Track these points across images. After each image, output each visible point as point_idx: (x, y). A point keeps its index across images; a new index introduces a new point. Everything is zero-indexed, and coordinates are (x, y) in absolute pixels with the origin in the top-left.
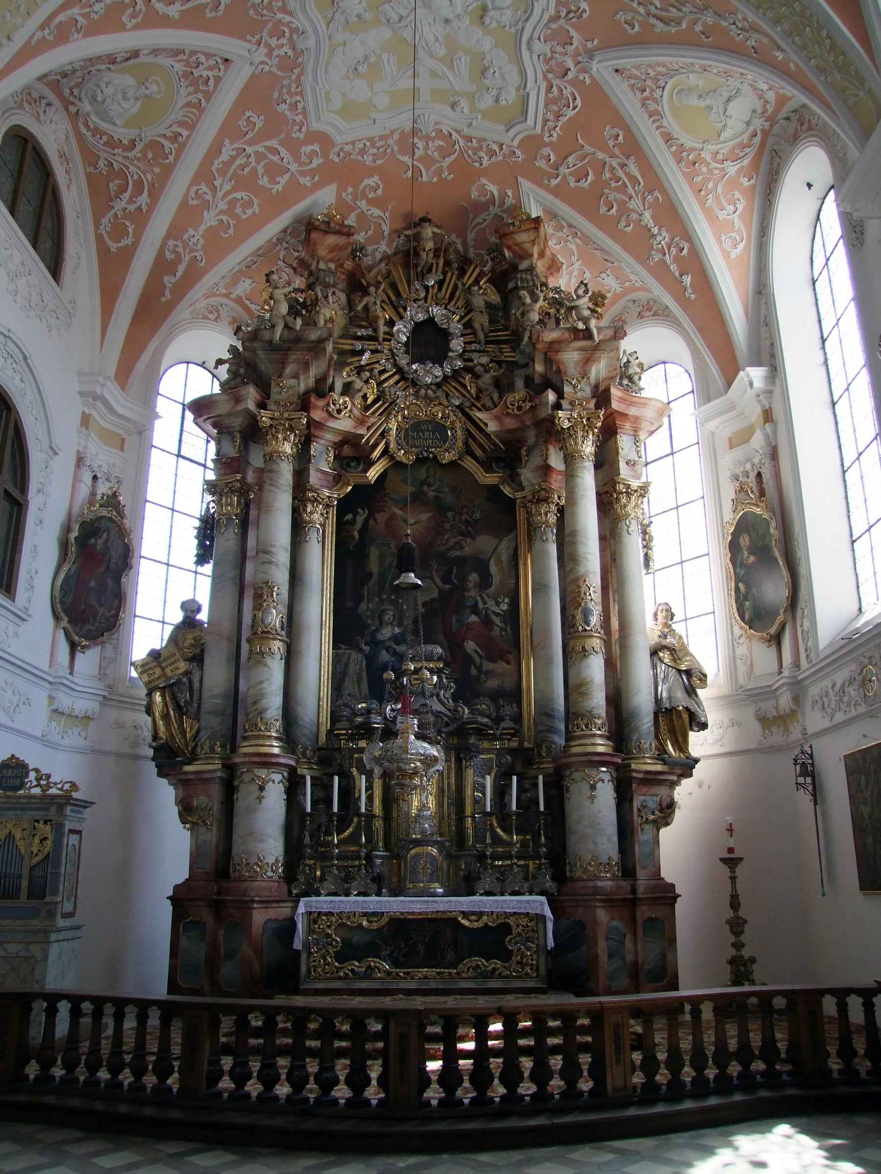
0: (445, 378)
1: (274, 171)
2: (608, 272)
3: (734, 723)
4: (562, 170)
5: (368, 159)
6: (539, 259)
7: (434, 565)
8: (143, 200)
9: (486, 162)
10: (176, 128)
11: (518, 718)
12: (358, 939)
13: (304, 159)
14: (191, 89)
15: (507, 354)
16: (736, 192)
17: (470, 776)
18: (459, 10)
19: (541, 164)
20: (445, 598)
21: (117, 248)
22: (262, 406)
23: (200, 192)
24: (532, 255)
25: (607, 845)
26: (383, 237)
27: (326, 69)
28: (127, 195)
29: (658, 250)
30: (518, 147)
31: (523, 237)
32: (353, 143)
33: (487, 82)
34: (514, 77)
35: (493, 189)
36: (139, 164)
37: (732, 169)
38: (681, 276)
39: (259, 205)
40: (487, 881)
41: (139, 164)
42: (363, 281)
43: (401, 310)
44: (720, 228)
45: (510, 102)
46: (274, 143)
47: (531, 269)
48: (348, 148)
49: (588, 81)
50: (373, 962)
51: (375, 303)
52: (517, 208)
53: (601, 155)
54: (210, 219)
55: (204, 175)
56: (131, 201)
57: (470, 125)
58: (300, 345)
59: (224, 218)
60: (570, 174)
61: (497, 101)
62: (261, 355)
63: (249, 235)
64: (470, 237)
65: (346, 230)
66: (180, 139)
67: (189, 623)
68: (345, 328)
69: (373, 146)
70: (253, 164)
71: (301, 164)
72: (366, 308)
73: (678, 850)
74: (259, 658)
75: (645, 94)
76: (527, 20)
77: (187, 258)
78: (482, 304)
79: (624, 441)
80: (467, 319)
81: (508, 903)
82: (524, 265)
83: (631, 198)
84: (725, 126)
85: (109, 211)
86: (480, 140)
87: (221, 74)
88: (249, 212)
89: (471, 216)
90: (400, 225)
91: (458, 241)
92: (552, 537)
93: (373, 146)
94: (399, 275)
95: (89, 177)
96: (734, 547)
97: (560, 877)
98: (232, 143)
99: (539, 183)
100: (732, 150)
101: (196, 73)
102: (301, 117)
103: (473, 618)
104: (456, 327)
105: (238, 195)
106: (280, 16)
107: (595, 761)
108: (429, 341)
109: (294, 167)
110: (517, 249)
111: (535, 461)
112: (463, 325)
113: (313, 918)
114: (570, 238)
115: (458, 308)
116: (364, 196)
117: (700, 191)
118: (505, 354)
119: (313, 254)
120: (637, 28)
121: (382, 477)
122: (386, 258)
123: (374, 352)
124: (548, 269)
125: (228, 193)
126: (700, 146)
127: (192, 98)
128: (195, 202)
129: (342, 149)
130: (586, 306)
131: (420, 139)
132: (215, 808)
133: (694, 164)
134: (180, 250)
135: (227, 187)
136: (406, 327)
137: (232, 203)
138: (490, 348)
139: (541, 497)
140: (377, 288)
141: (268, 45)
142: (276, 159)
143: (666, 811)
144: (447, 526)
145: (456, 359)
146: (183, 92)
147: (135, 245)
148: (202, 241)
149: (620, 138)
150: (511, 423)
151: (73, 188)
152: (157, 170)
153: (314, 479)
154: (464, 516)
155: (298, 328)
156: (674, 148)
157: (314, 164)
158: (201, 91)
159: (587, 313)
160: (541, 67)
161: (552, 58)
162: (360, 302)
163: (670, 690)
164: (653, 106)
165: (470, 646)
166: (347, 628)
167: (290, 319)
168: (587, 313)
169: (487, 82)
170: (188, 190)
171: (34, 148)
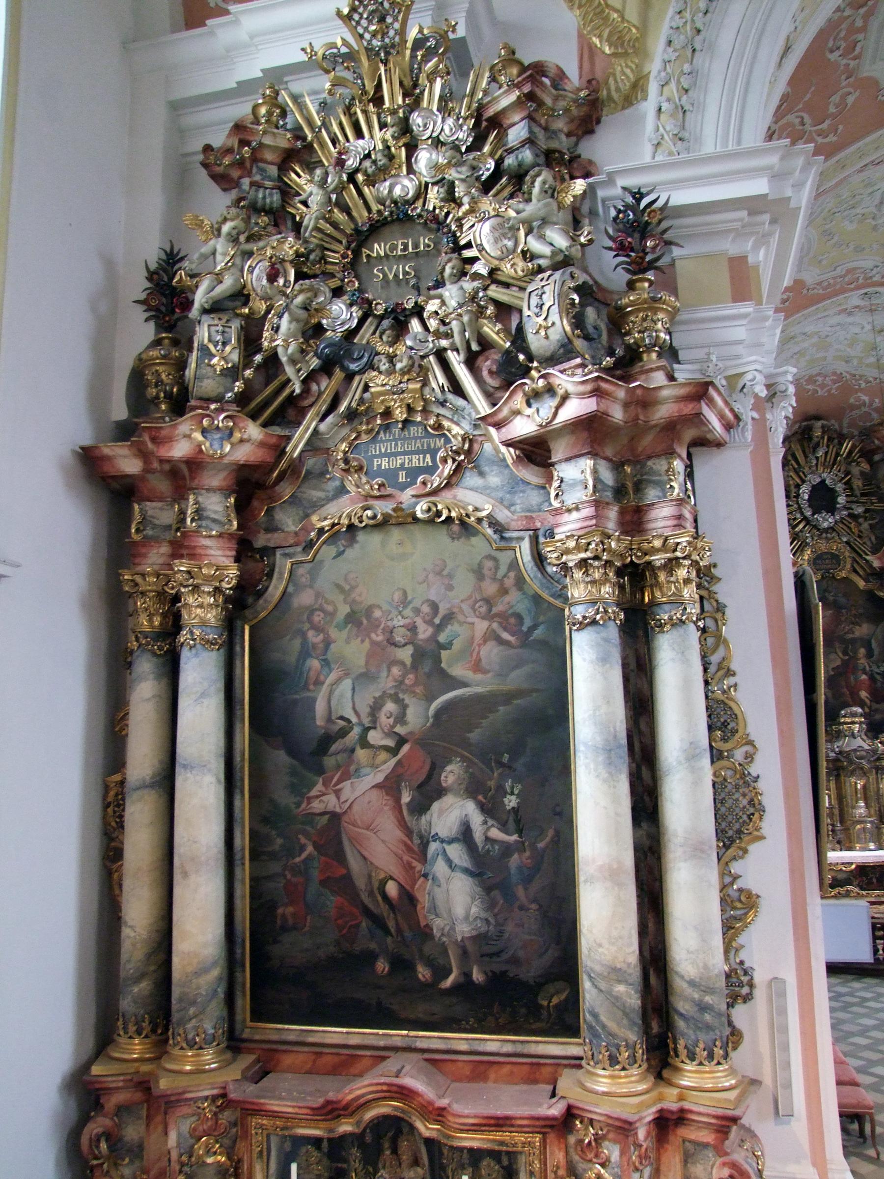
0: (836, 522)
7: (837, 645)
9: (863, 385)
12: (840, 876)
20: (845, 664)
35: (866, 399)
50: (849, 887)
86: (861, 376)
103: (864, 677)
104: (840, 487)
144: (843, 619)
154: (854, 612)
165: (864, 694)
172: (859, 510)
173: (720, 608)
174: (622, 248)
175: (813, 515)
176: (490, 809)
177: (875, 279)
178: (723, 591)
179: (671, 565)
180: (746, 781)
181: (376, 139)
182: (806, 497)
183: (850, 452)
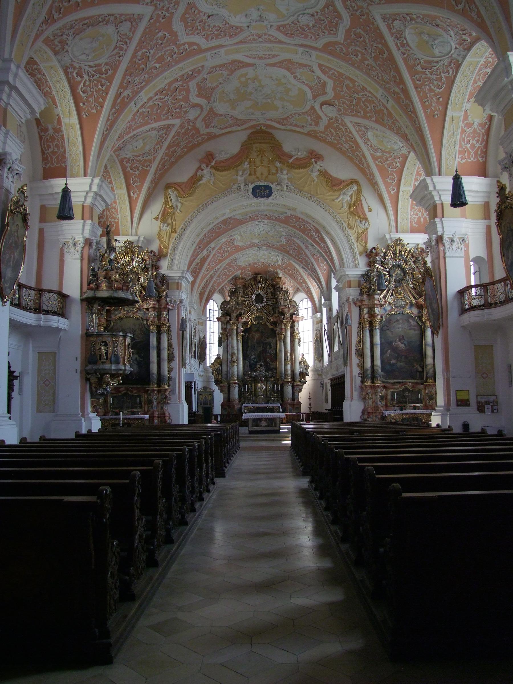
3: (314, 375)
8: (208, 283)
11: (276, 373)
15: (275, 302)
17: (268, 385)
22: (230, 320)
25: (290, 396)
31: (278, 280)
40: (271, 401)
47: (279, 287)
52: (277, 273)
54: (218, 282)
55: (219, 276)
64: (268, 276)
67: (218, 358)
73: (303, 396)
74: (233, 366)
79: (296, 324)
81: (274, 405)
82: (278, 286)
92: (283, 341)
96: (315, 343)
97: (282, 401)
104: (265, 296)
107: (288, 382)
108: (259, 299)
111: (280, 327)
113: (245, 407)
119: (237, 283)
121: (251, 326)
132: (226, 390)
139: (281, 334)
143: (300, 390)
150: (275, 320)
153: (239, 331)
163: (303, 369)
165: (268, 359)
166: (245, 357)
172: (270, 303)
173: (171, 331)
174: (160, 282)
176: (140, 356)
178: (171, 329)
179: (163, 325)
180: (173, 353)
181: (127, 259)
183: (269, 285)
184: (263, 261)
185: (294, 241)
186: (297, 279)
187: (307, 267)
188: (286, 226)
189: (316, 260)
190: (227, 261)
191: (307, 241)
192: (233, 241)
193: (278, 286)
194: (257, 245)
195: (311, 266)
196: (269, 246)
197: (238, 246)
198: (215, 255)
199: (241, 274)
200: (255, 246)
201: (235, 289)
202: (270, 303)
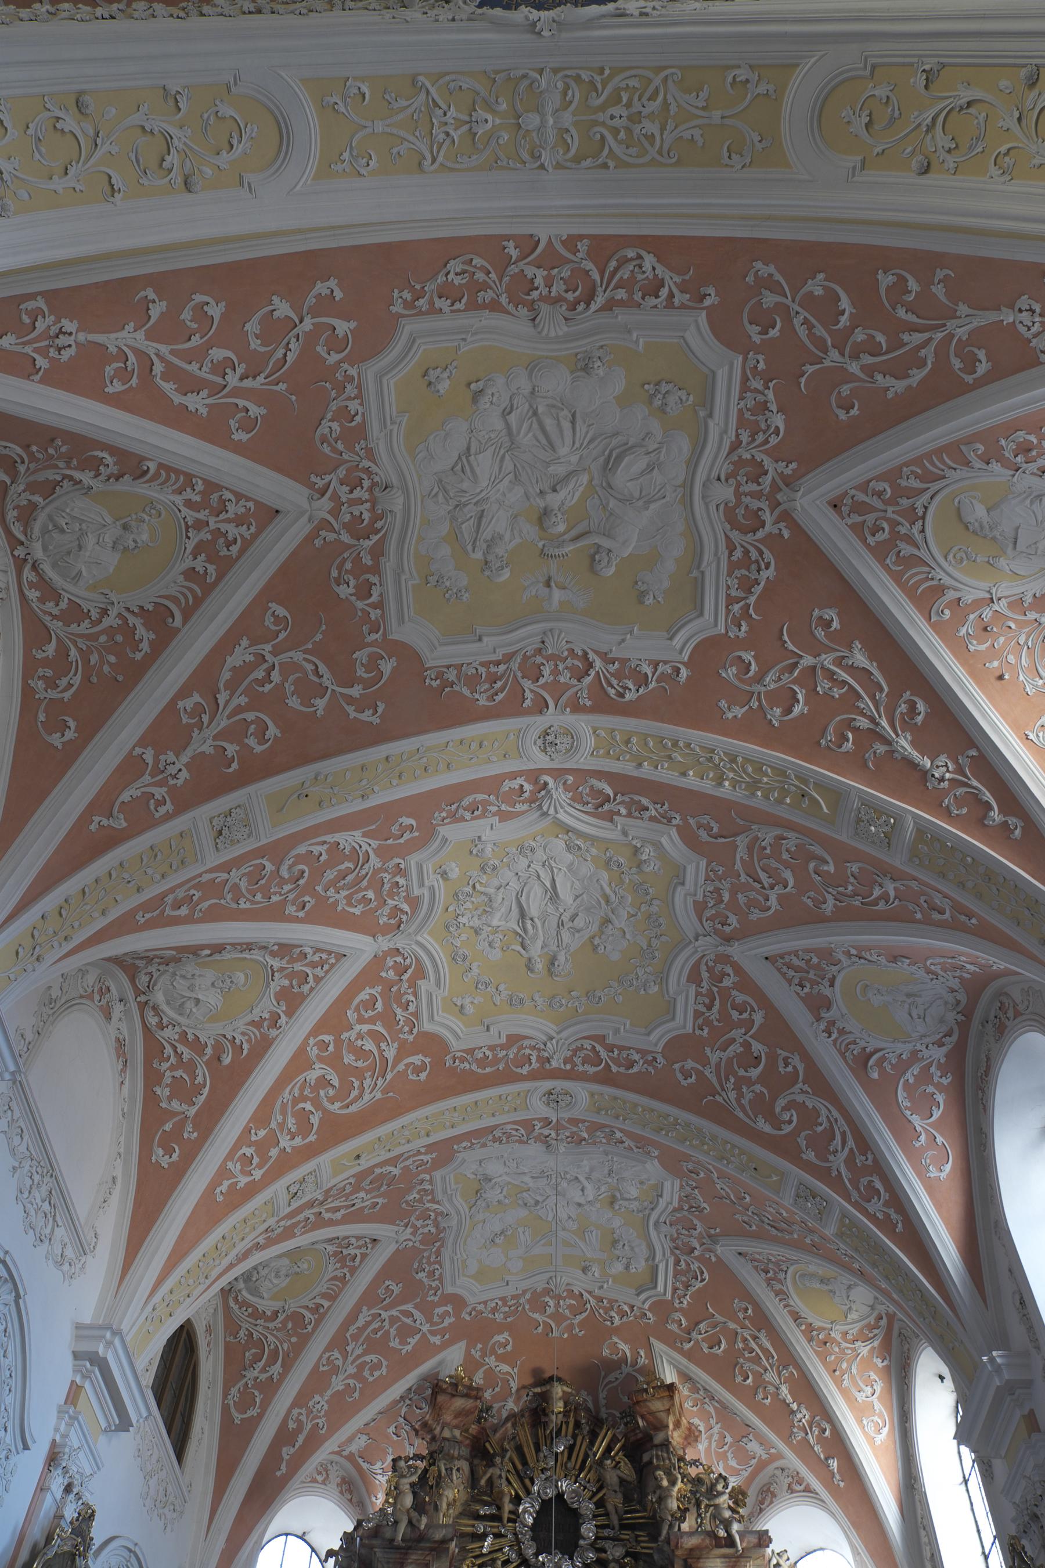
1: (406, 1332)
2: (751, 1437)
4: (694, 1334)
5: (500, 1317)
6: (674, 1429)
8: (276, 1369)
9: (617, 1321)
10: (318, 1300)
13: (436, 1319)
14: (338, 1265)
15: (645, 1546)
16: (872, 1373)
18: (591, 1198)
19: (673, 1327)
21: (242, 1419)
23: (332, 1358)
24: (667, 1426)
26: (511, 1394)
27: (465, 1241)
28: (261, 1364)
29: (799, 1427)
30: (649, 1310)
31: (657, 1405)
32: (485, 1303)
33: (617, 1252)
34: (643, 1251)
36: (278, 1334)
37: (864, 1350)
38: (827, 1459)
39: (387, 1367)
41: (278, 1334)
42: (487, 1445)
43: (527, 1482)
44: (861, 1411)
45: (640, 1270)
46: (409, 1307)
47: (666, 1445)
48: (481, 1307)
49: (713, 1259)
51: (500, 1476)
52: (650, 1372)
53: (732, 1326)
54: (337, 1384)
55: (339, 1342)
56: (264, 1370)
57: (601, 1287)
58: (422, 1545)
59: (351, 1381)
60: (703, 1340)
61: (627, 1267)
62: (379, 1553)
63: (374, 1396)
64: (602, 1395)
65: (474, 1393)
66: (322, 1310)
68: (466, 1504)
69: (505, 1304)
70: (387, 1327)
71: (433, 1324)
72: (490, 1482)
75: (769, 1275)
76: (653, 1209)
77: (310, 1426)
78: (616, 1480)
80: (600, 1495)
83: (766, 1370)
84: (850, 1308)
85: (240, 1380)
86: (610, 1301)
87: (368, 1252)
88: (377, 1374)
89: (603, 1373)
90: (529, 1380)
91: (589, 1399)
93: (505, 1304)
94: (525, 1436)
95: (228, 1347)
98: (368, 1310)
99: (672, 1345)
100: (861, 1330)
101: (345, 1252)
102: (437, 1282)
104: (588, 1507)
105: (368, 1358)
106: (428, 1205)
108: (558, 1524)
109: (425, 1328)
110: (651, 1418)
112: (595, 1503)
114: (707, 1400)
115: (589, 1482)
116: (493, 1352)
117: (834, 1371)
118: (643, 1545)
120: (754, 1228)
122: (512, 1416)
123: (497, 1536)
124: (686, 1438)
125: (359, 1357)
126: (829, 1326)
127: (338, 1273)
128: (325, 1368)
129: (474, 1309)
130: (726, 1505)
131: (551, 1298)
133: (825, 1343)
134: (303, 1418)
135: (359, 1351)
136: (533, 1506)
137: (361, 1367)
138: (626, 1535)
140: (503, 1457)
141: (414, 1226)
142: (409, 1321)
145: (587, 1550)
146: (330, 1268)
147: (260, 1416)
148: (326, 1407)
149: (750, 1311)
151: (211, 1357)
152: (294, 1340)
155: (422, 1527)
156: (803, 1327)
157: (446, 1323)
158: (347, 1266)
159: (727, 1514)
160: (668, 1244)
161: (678, 1238)
162: (485, 1473)
164: (778, 1286)
167: (414, 1515)
168: (727, 1514)
169: (617, 1252)
170: (321, 1357)
171: (188, 1333)
175: (537, 1555)
177: (554, 1064)
182: (530, 1521)
183: (609, 1449)
184: (580, 1283)
185: (746, 984)
186: (760, 1383)
187: (824, 1174)
188: (698, 737)
189: (882, 1095)
190: (370, 1147)
191: (837, 796)
192: (413, 984)
193: (659, 1438)
194: (544, 1073)
195: (850, 1161)
196: (606, 1078)
197: (432, 1045)
198: (299, 1062)
199: (471, 1364)
200: (534, 1076)
201: (431, 1454)
202: (615, 1552)
